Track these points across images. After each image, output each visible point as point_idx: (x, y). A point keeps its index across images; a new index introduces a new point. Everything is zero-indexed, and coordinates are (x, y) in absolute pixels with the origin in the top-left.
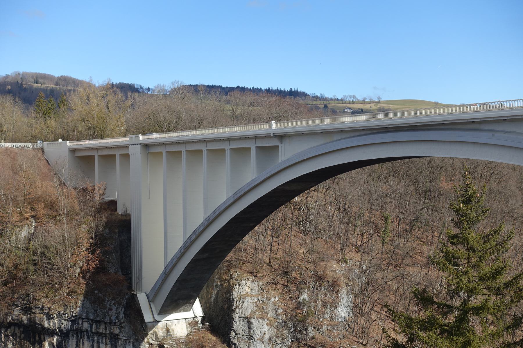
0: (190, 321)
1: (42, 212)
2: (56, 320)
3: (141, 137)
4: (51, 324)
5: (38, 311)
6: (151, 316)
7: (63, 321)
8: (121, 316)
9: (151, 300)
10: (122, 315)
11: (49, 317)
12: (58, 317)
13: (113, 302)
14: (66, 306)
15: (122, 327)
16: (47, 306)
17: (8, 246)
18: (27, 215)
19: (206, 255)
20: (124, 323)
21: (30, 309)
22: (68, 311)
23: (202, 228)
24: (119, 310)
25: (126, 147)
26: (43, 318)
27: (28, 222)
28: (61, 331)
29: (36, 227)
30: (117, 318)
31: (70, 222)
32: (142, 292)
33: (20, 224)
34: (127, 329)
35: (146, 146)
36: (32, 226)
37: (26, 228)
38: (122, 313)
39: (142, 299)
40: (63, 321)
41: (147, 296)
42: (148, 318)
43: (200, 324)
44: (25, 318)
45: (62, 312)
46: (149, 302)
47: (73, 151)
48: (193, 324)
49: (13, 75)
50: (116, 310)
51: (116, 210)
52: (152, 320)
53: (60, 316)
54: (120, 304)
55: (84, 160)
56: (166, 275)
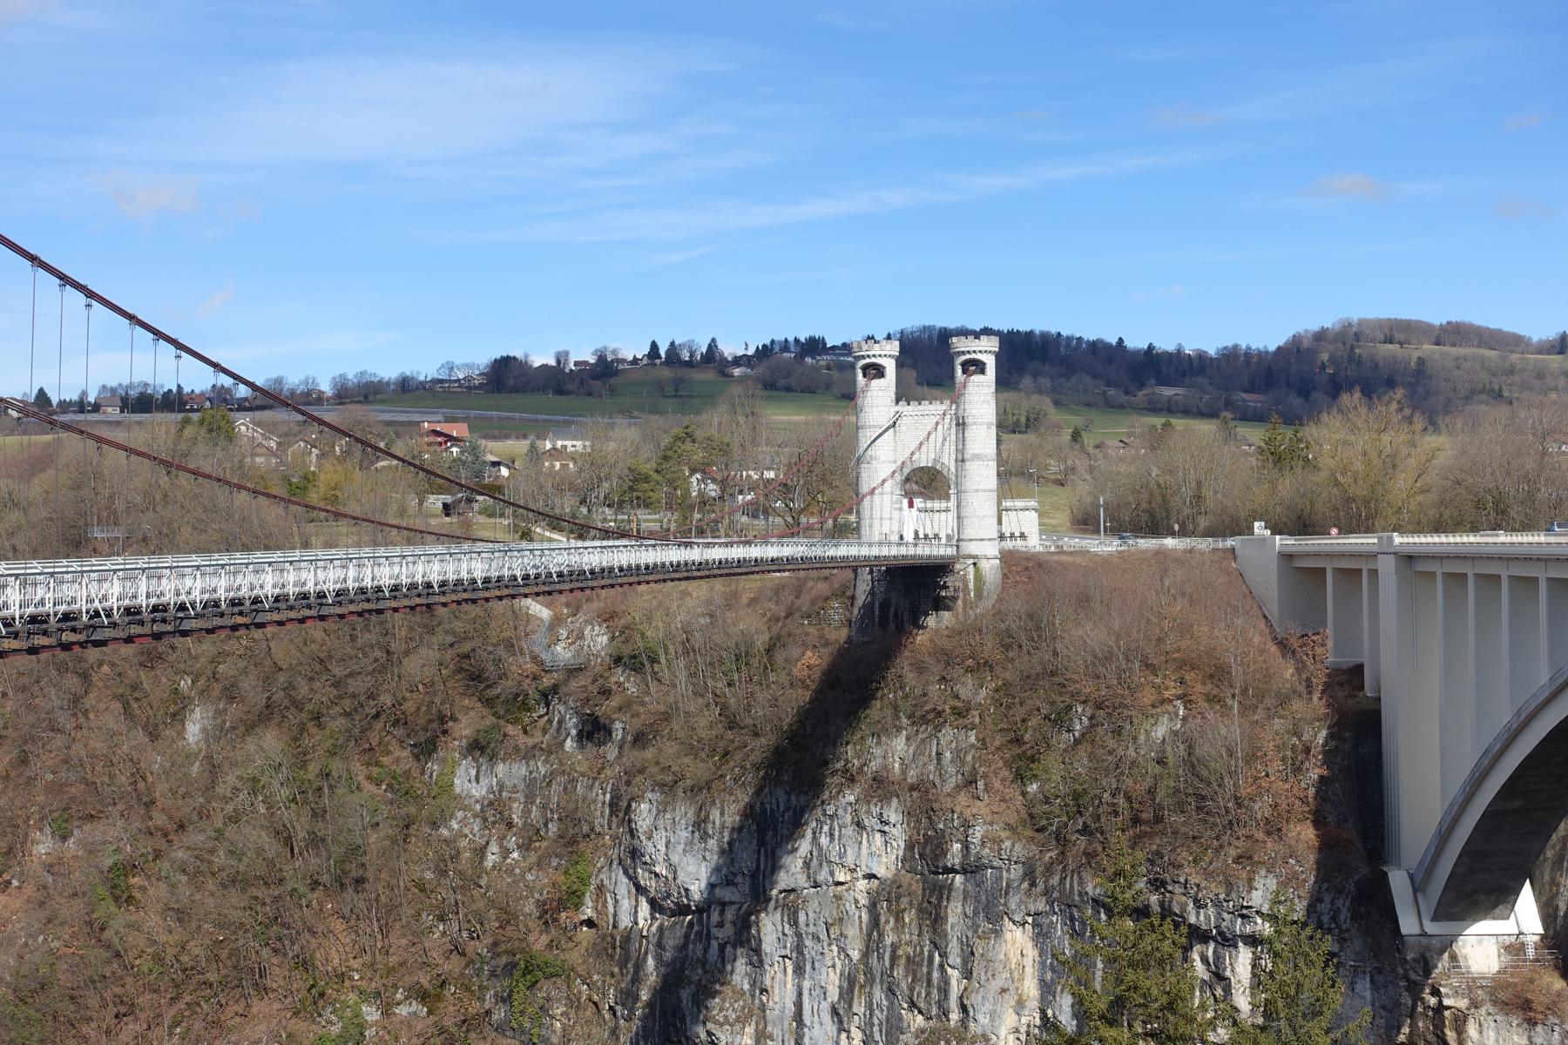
0: (1508, 941)
1: (1199, 688)
2: (1211, 911)
3: (1398, 539)
4: (1202, 918)
5: (1178, 889)
6: (1416, 923)
7: (1225, 915)
8: (1342, 917)
9: (1418, 886)
10: (1344, 915)
11: (1199, 905)
12: (1215, 905)
13: (1326, 885)
14: (1229, 886)
15: (1345, 940)
16: (1193, 880)
17: (1131, 752)
18: (1167, 694)
19: (1517, 804)
20: (1348, 931)
21: (1164, 883)
22: (1234, 896)
23: (1498, 746)
24: (1339, 903)
25: (1372, 556)
26: (1186, 904)
27: (1170, 708)
28: (1221, 933)
29: (1184, 719)
30: (1334, 919)
31: (1245, 709)
32: (1399, 867)
33: (1153, 711)
34: (1357, 944)
35: (1408, 559)
36: (1177, 715)
37: (1166, 719)
38: (1344, 911)
39: (1398, 881)
40: (1225, 915)
41: (1411, 877)
42: (1408, 924)
43: (1531, 953)
44: (1154, 899)
45: (1222, 896)
46: (1415, 891)
47: (1287, 557)
48: (1515, 948)
49: (1338, 327)
50: (1332, 903)
51: (1362, 687)
52: (1417, 931)
53: (1218, 904)
54: (1340, 891)
55: (1304, 577)
56: (1443, 837)
